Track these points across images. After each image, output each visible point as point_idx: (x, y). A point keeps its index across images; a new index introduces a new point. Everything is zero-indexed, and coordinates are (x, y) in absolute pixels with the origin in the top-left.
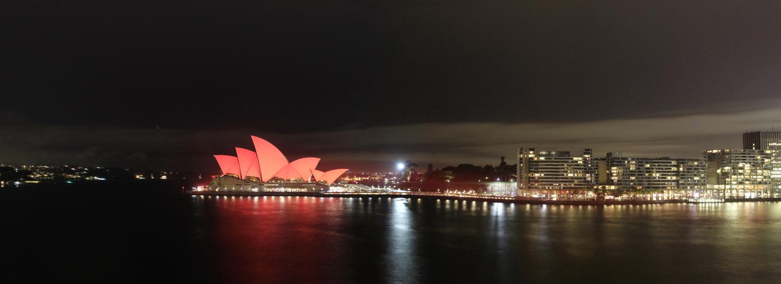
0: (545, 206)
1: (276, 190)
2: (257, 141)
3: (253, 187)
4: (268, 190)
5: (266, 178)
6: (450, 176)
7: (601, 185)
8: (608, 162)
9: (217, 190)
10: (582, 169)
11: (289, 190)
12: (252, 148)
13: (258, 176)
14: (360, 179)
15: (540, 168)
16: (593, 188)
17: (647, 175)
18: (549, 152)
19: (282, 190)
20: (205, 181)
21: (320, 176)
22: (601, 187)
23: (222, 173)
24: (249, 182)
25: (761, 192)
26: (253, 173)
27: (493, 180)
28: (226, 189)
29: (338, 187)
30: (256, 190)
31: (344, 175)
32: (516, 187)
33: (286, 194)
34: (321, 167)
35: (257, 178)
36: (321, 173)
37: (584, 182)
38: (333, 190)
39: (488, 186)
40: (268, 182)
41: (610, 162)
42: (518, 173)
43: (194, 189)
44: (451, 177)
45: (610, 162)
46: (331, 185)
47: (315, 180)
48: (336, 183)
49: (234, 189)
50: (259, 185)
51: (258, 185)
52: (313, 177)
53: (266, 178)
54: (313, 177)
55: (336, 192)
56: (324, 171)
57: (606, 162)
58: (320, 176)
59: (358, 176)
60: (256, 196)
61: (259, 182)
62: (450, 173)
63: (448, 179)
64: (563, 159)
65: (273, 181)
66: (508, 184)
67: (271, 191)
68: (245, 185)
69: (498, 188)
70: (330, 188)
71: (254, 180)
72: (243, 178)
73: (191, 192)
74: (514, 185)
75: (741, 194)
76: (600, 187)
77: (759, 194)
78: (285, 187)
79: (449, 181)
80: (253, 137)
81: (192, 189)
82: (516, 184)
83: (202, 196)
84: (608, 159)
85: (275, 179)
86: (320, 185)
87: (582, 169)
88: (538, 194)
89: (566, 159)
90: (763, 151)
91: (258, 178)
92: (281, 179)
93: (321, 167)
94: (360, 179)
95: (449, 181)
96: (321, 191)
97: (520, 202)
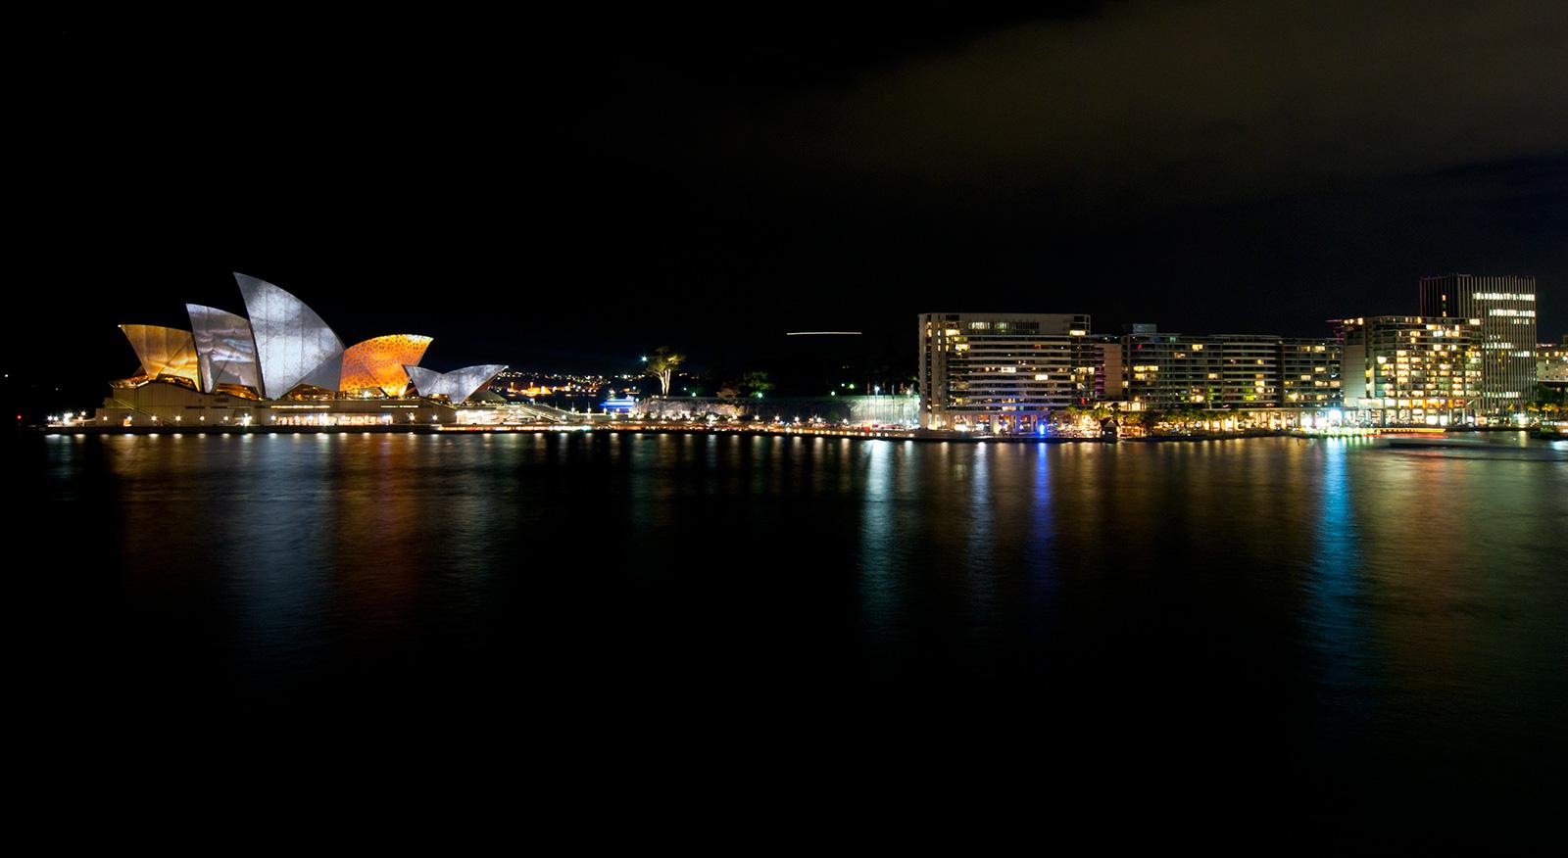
0: (945, 445)
1: (310, 420)
3: (239, 413)
4: (284, 421)
6: (765, 382)
7: (1110, 400)
8: (1125, 347)
9: (127, 422)
10: (1065, 363)
11: (344, 420)
13: (254, 383)
14: (544, 391)
15: (971, 362)
16: (1091, 408)
17: (1212, 376)
18: (992, 324)
19: (325, 420)
20: (89, 399)
22: (1110, 404)
24: (226, 400)
25: (1460, 415)
27: (863, 391)
28: (154, 418)
29: (481, 413)
30: (246, 421)
32: (919, 407)
35: (249, 388)
37: (1072, 393)
38: (466, 418)
39: (854, 404)
42: (922, 372)
43: (52, 422)
44: (766, 386)
46: (463, 407)
47: (416, 393)
48: (476, 400)
49: (178, 418)
50: (256, 407)
51: (252, 408)
57: (1120, 347)
59: (538, 384)
60: (245, 433)
62: (764, 376)
63: (758, 389)
64: (1023, 339)
65: (299, 397)
66: (898, 401)
67: (291, 423)
68: (212, 407)
69: (875, 409)
71: (242, 395)
73: (44, 429)
74: (912, 402)
76: (1108, 405)
78: (331, 412)
79: (760, 395)
81: (48, 422)
82: (917, 400)
83: (80, 436)
84: (1126, 339)
87: (1065, 363)
88: (968, 423)
89: (1031, 339)
93: (437, 361)
94: (544, 391)
95: (760, 395)
96: (433, 422)
97: (924, 438)
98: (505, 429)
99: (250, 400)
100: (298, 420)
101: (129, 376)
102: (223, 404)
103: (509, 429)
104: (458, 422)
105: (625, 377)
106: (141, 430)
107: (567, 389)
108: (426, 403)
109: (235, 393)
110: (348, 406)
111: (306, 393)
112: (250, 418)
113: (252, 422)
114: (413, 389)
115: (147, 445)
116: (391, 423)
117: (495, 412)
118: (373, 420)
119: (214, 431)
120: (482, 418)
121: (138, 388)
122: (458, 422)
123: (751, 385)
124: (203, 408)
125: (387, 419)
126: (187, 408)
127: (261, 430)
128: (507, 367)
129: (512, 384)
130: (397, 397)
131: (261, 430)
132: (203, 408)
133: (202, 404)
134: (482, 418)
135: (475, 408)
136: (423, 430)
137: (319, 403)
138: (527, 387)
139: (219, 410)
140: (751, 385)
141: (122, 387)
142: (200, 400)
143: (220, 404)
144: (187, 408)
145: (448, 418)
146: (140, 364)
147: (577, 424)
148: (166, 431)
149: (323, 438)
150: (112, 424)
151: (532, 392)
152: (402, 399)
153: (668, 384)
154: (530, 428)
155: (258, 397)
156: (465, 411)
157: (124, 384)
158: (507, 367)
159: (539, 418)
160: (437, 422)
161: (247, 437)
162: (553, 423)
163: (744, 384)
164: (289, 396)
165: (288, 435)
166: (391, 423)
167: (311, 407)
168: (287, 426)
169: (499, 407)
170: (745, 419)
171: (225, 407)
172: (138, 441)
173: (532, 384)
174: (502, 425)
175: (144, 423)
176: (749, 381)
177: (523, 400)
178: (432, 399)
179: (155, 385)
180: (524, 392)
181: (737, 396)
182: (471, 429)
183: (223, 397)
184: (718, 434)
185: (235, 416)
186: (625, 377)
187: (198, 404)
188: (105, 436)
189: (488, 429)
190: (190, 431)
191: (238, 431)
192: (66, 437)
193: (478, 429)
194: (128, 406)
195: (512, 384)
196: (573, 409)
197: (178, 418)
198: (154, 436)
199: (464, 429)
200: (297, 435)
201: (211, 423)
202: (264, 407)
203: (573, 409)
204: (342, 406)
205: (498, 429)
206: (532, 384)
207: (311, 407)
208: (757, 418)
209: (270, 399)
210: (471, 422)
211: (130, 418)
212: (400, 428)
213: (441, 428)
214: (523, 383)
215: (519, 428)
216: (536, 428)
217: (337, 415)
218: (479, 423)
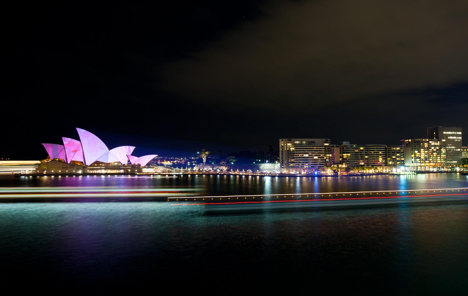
0: (287, 178)
1: (99, 171)
2: (81, 132)
3: (78, 169)
4: (91, 172)
5: (89, 163)
6: (234, 159)
7: (336, 164)
8: (340, 148)
9: (45, 172)
10: (323, 153)
11: (109, 171)
12: (77, 138)
13: (82, 160)
15: (295, 153)
16: (331, 167)
17: (366, 157)
18: (301, 142)
19: (103, 171)
21: (135, 160)
22: (336, 165)
23: (50, 158)
24: (74, 166)
26: (78, 158)
27: (263, 162)
28: (53, 171)
29: (150, 169)
30: (80, 172)
31: (154, 159)
32: (280, 167)
33: (106, 174)
34: (134, 154)
36: (136, 158)
37: (325, 162)
38: (145, 170)
39: (260, 166)
40: (91, 165)
41: (342, 148)
42: (280, 156)
45: (342, 148)
46: (145, 167)
47: (130, 163)
49: (60, 171)
50: (83, 168)
51: (82, 168)
52: (129, 161)
53: (89, 163)
54: (129, 161)
55: (148, 172)
56: (138, 157)
57: (339, 148)
58: (135, 160)
59: (167, 160)
60: (80, 175)
61: (83, 166)
62: (234, 157)
63: (232, 162)
64: (310, 146)
65: (96, 165)
66: (273, 165)
67: (93, 172)
68: (70, 168)
69: (267, 167)
70: (143, 169)
71: (79, 164)
72: (69, 162)
74: (278, 165)
75: (427, 169)
76: (335, 166)
77: (438, 169)
78: (105, 169)
79: (233, 163)
80: (76, 128)
82: (279, 164)
84: (341, 146)
85: (97, 163)
86: (135, 167)
87: (323, 153)
88: (294, 171)
89: (312, 146)
90: (440, 140)
91: (82, 162)
92: (102, 163)
95: (233, 163)
97: (281, 176)
98: (157, 174)
99: (81, 166)
100: (95, 172)
101: (45, 159)
102: (73, 167)
103: (158, 174)
104: (143, 172)
105: (193, 158)
106: (49, 175)
107: (175, 162)
108: (134, 167)
109: (77, 164)
110: (110, 167)
111: (98, 163)
112: (81, 171)
113: (82, 172)
114: (129, 162)
115: (51, 179)
116: (123, 172)
117: (154, 169)
118: (118, 172)
119: (71, 175)
120: (150, 170)
121: (48, 162)
122: (143, 172)
123: (230, 160)
124: (67, 168)
125: (122, 171)
126: (62, 168)
127: (84, 174)
128: (157, 155)
129: (159, 160)
130: (124, 164)
131: (84, 174)
132: (67, 168)
133: (67, 167)
134: (150, 170)
135: (148, 168)
136: (133, 174)
137: (102, 166)
138: (163, 161)
139: (72, 169)
140: (230, 160)
141: (43, 162)
142: (66, 166)
143: (72, 167)
144: (62, 168)
145: (140, 170)
146: (49, 155)
147: (178, 172)
148: (56, 175)
149: (103, 177)
150: (40, 173)
151: (165, 163)
152: (126, 165)
153: (205, 160)
154: (164, 173)
155: (84, 165)
156: (145, 168)
157: (44, 161)
158: (157, 155)
159: (167, 170)
160: (136, 172)
161: (80, 177)
162: (171, 172)
163: (228, 160)
164: (93, 164)
165: (93, 176)
166: (123, 172)
167: (99, 168)
168: (92, 173)
169: (155, 167)
170: (228, 170)
171: (74, 168)
172: (48, 178)
173: (165, 160)
174: (156, 172)
175: (50, 172)
176: (229, 159)
177: (162, 165)
178: (135, 165)
179: (53, 161)
180: (163, 163)
181: (226, 164)
182: (147, 174)
183: (73, 165)
184: (220, 175)
185: (77, 170)
186: (193, 158)
187: (66, 167)
188: (38, 177)
189: (152, 174)
190: (63, 175)
191: (78, 175)
192: (27, 178)
193: (149, 174)
194: (45, 168)
195: (159, 160)
196: (177, 168)
197: (60, 171)
198: (53, 177)
199: (145, 174)
200: (95, 176)
201: (69, 173)
202: (85, 168)
203: (177, 168)
204: (109, 167)
205: (155, 174)
206: (165, 160)
207: (99, 168)
208: (232, 170)
209: (87, 165)
210: (147, 172)
211: (45, 171)
212: (126, 174)
213: (138, 174)
214: (162, 160)
215: (161, 174)
216: (166, 174)
217: (107, 170)
218: (149, 172)
